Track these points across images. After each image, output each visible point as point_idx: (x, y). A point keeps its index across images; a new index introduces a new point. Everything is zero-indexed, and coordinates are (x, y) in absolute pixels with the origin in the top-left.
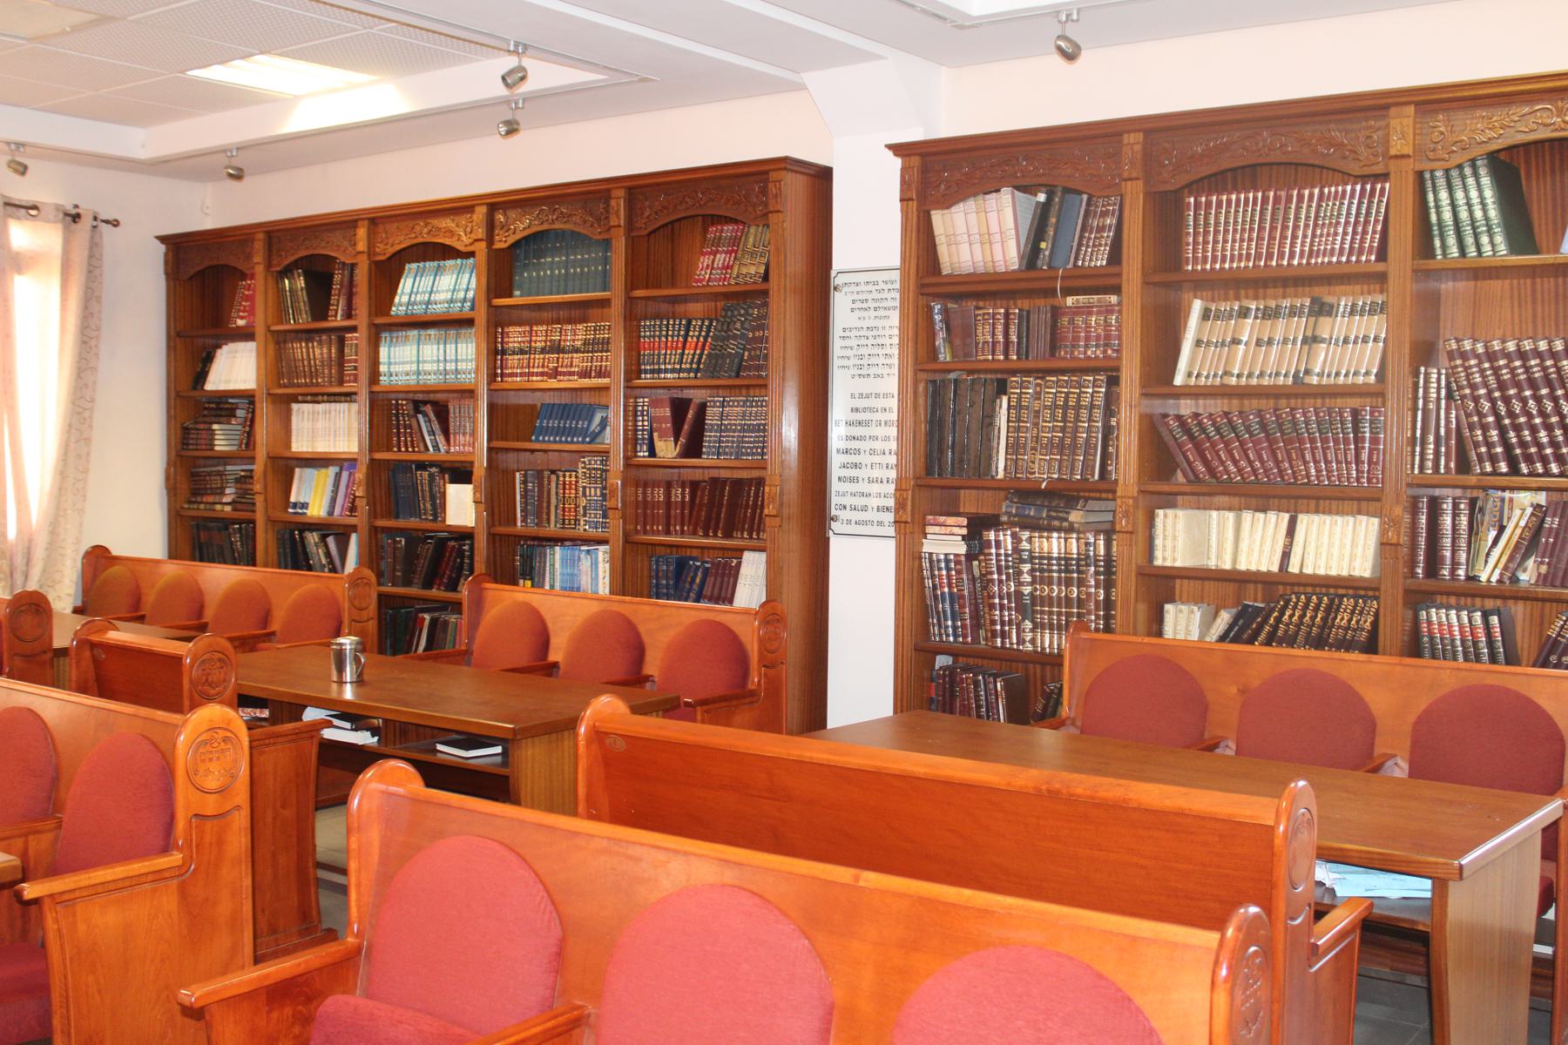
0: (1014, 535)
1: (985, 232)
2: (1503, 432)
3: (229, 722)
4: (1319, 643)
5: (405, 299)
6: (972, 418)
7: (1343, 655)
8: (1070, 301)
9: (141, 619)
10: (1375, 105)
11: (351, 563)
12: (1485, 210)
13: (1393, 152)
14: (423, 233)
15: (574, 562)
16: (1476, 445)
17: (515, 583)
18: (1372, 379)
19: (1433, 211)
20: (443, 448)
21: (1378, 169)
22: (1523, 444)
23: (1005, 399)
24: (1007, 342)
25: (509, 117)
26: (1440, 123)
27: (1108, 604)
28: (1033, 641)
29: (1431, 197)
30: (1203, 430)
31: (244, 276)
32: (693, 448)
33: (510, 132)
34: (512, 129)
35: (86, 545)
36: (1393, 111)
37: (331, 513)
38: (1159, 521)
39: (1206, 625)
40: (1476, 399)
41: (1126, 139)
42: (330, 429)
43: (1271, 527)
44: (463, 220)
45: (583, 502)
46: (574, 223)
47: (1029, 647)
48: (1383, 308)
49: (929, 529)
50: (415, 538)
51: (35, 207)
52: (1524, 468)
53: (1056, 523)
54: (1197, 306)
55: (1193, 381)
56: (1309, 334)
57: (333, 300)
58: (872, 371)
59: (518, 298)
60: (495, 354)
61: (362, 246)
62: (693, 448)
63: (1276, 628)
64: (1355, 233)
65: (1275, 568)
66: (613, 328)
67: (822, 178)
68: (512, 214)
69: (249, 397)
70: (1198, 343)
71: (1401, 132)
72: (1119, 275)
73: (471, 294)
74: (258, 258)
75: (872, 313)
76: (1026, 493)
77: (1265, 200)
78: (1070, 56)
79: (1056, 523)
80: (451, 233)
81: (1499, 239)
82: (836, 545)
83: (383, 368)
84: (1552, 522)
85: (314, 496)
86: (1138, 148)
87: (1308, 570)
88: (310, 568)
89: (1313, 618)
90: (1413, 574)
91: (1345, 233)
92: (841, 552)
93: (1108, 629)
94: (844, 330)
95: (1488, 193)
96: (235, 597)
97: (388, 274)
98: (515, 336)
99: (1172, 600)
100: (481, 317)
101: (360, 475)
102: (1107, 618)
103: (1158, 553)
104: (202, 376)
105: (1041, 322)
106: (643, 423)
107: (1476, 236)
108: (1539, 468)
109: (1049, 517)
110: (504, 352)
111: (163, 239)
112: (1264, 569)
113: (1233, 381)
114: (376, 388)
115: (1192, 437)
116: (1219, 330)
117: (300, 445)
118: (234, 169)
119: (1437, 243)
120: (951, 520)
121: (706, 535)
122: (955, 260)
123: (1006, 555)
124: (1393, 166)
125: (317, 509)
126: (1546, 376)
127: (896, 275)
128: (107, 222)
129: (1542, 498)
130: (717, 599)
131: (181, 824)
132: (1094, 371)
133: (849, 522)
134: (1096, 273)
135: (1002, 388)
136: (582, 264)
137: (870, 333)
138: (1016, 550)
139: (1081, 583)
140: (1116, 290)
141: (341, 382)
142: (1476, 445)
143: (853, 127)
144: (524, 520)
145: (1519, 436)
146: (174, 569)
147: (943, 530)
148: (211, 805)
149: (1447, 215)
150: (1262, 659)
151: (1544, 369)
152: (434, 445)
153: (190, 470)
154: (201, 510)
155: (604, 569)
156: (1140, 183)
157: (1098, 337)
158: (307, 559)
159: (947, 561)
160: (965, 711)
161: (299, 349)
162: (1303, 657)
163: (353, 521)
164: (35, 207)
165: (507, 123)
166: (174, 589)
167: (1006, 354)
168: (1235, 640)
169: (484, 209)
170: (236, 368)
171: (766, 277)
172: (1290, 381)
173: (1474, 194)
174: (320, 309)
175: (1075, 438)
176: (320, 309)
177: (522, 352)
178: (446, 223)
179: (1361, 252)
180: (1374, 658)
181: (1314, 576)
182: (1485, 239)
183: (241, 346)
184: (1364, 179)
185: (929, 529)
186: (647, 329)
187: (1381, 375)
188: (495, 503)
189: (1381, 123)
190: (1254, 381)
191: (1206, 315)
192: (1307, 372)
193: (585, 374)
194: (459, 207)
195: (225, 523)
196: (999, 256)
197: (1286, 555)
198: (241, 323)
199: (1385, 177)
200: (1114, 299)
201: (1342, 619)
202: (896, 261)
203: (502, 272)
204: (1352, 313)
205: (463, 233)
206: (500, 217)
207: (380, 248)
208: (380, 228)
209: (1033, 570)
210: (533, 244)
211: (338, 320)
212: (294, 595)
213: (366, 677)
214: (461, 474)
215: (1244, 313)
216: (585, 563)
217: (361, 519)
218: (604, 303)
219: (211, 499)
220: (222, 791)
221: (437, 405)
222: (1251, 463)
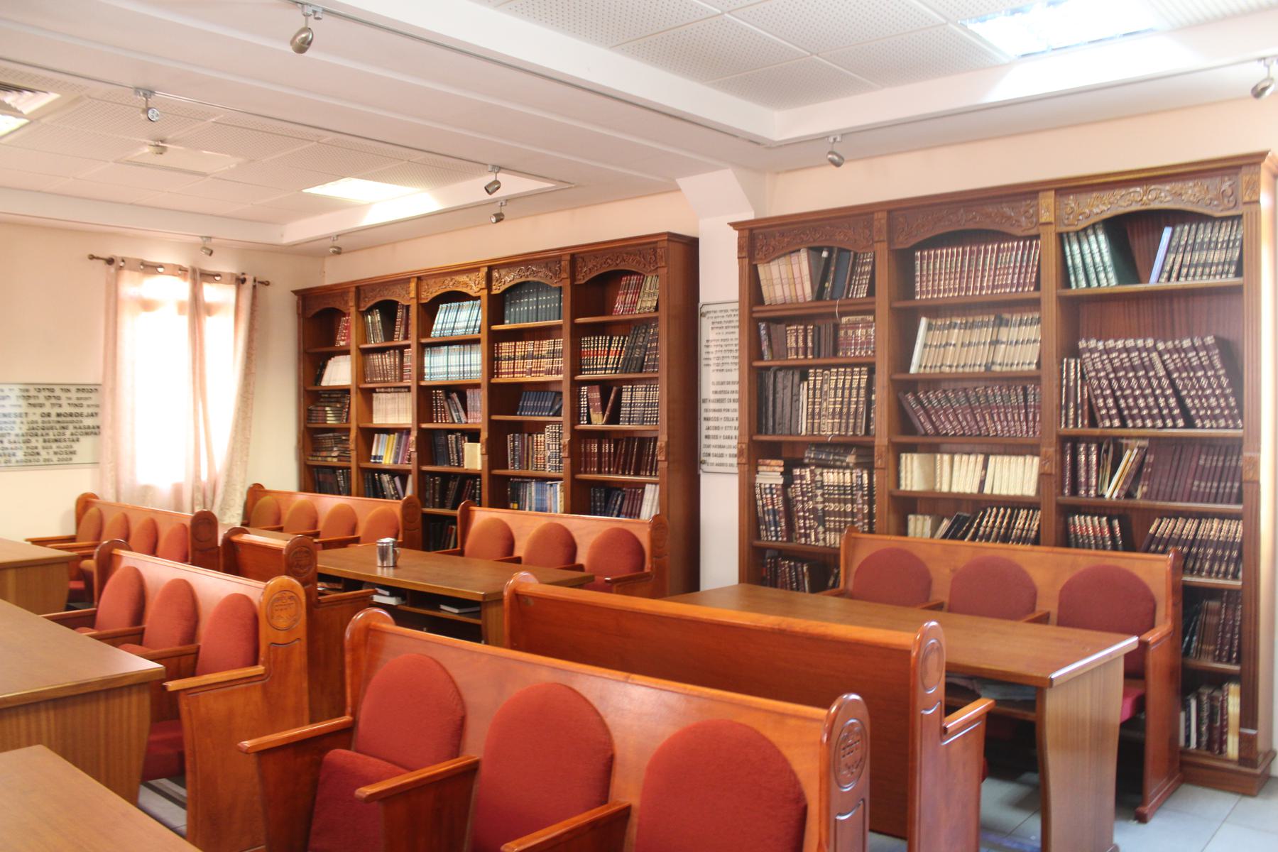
0: (812, 472)
1: (789, 279)
2: (1116, 400)
3: (293, 586)
4: (1005, 538)
5: (439, 327)
6: (784, 396)
7: (1020, 546)
8: (844, 320)
9: (281, 530)
10: (1027, 193)
11: (409, 492)
13: (1043, 220)
14: (450, 285)
15: (541, 492)
16: (1099, 409)
17: (507, 507)
18: (1033, 367)
20: (464, 420)
21: (1033, 232)
22: (1129, 408)
25: (498, 211)
26: (1071, 201)
27: (871, 515)
28: (824, 539)
29: (1067, 249)
31: (344, 315)
32: (614, 418)
33: (497, 221)
34: (500, 218)
35: (250, 483)
36: (1041, 195)
37: (396, 462)
38: (903, 460)
39: (935, 528)
41: (876, 216)
42: (395, 411)
43: (972, 465)
44: (473, 276)
45: (548, 453)
46: (541, 276)
47: (821, 543)
48: (1039, 321)
49: (760, 468)
50: (446, 476)
51: (218, 275)
52: (1130, 423)
54: (924, 322)
55: (922, 370)
57: (397, 328)
58: (725, 367)
59: (507, 326)
60: (492, 362)
61: (413, 294)
62: (614, 418)
63: (977, 529)
64: (1020, 273)
65: (975, 491)
66: (563, 343)
67: (690, 246)
68: (503, 272)
69: (345, 391)
70: (925, 346)
71: (1047, 207)
72: (873, 303)
73: (478, 323)
74: (352, 303)
75: (725, 330)
76: (820, 445)
77: (964, 253)
78: (837, 165)
80: (467, 285)
81: (1111, 275)
82: (705, 481)
83: (427, 371)
84: (1150, 458)
85: (385, 453)
86: (884, 221)
87: (996, 492)
88: (384, 497)
89: (1002, 523)
90: (1063, 494)
91: (1014, 273)
92: (709, 485)
93: (871, 531)
95: (1104, 246)
96: (338, 513)
97: (429, 311)
98: (506, 348)
99: (915, 512)
100: (484, 337)
101: (413, 438)
102: (871, 524)
103: (903, 482)
104: (320, 377)
105: (827, 330)
106: (584, 403)
107: (1097, 274)
108: (1139, 422)
110: (499, 359)
111: (296, 292)
112: (968, 491)
113: (947, 370)
114: (423, 383)
115: (923, 407)
116: (938, 337)
117: (378, 420)
118: (337, 248)
119: (1072, 278)
120: (774, 462)
121: (623, 474)
124: (1042, 230)
125: (387, 461)
126: (1143, 363)
127: (736, 306)
128: (262, 283)
129: (1145, 443)
130: (630, 515)
131: (263, 648)
132: (860, 365)
134: (861, 302)
136: (547, 302)
138: (813, 481)
139: (853, 502)
140: (872, 312)
141: (402, 379)
142: (1099, 409)
143: (712, 211)
144: (513, 464)
146: (304, 497)
148: (281, 638)
149: (1078, 260)
150: (966, 550)
151: (1141, 359)
152: (457, 419)
153: (312, 437)
154: (318, 461)
155: (560, 496)
156: (885, 245)
157: (862, 343)
158: (383, 491)
159: (771, 489)
160: (784, 586)
161: (376, 359)
162: (995, 549)
163: (409, 467)
164: (218, 275)
165: (496, 215)
166: (301, 509)
167: (805, 354)
168: (953, 537)
169: (486, 270)
170: (339, 373)
171: (657, 309)
172: (983, 369)
173: (1094, 246)
174: (389, 333)
175: (849, 409)
176: (389, 333)
177: (509, 359)
178: (463, 278)
179: (1024, 286)
180: (1036, 548)
181: (1000, 496)
182: (1102, 275)
183: (341, 358)
184: (1025, 238)
185: (760, 468)
186: (588, 343)
187: (1038, 364)
188: (496, 455)
189: (1034, 203)
190: (960, 370)
191: (929, 327)
192: (993, 363)
193: (549, 372)
194: (471, 269)
195: (334, 469)
196: (800, 293)
197: (982, 483)
198: (342, 343)
199: (1037, 237)
200: (870, 318)
201: (1020, 523)
202: (736, 297)
203: (497, 307)
205: (473, 285)
206: (495, 274)
207: (424, 295)
208: (424, 283)
209: (823, 495)
210: (515, 291)
211: (399, 341)
212: (372, 514)
213: (399, 563)
214: (473, 436)
216: (549, 493)
217: (412, 466)
218: (559, 327)
219: (325, 454)
220: (288, 630)
221: (458, 391)
222: (977, 423)
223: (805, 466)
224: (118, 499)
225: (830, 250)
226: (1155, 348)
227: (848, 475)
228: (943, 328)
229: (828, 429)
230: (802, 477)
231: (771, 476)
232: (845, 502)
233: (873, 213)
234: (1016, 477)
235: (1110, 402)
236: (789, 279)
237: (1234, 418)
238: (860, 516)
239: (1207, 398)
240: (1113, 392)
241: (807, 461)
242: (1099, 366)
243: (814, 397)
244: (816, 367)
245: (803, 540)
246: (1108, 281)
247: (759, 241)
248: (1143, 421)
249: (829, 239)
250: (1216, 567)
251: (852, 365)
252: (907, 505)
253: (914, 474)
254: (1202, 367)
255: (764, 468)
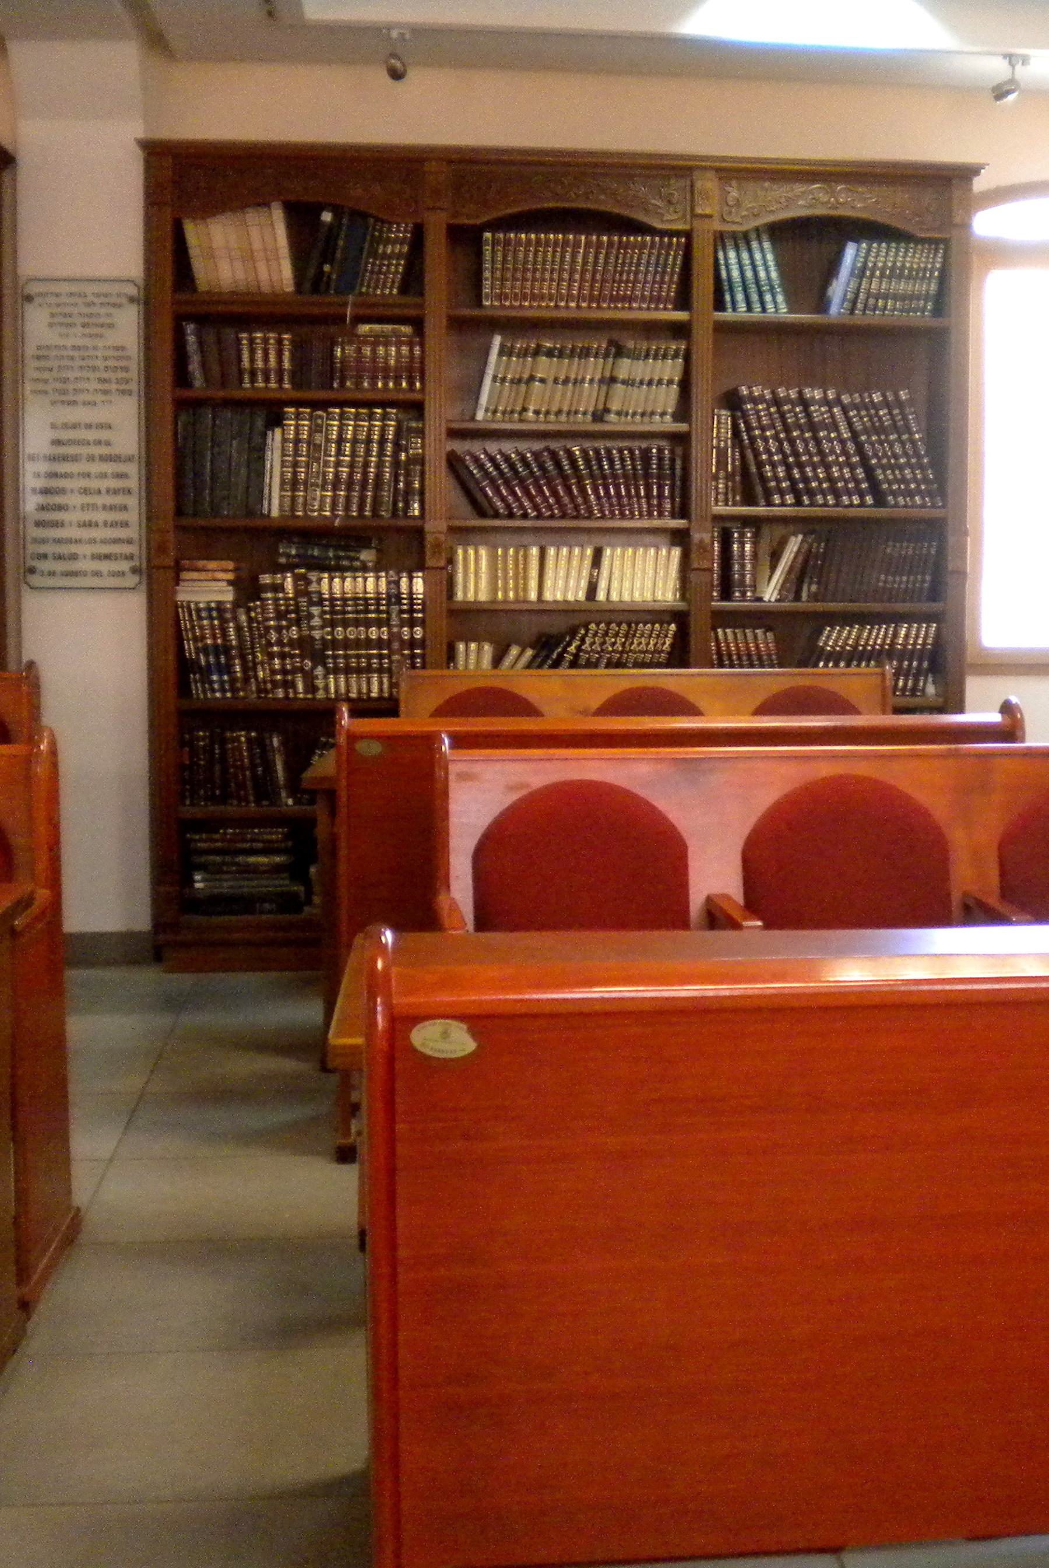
0: (297, 578)
1: (248, 252)
2: (789, 468)
8: (364, 328)
12: (768, 272)
19: (723, 267)
23: (278, 432)
24: (280, 371)
28: (326, 688)
30: (497, 467)
40: (766, 440)
41: (427, 167)
47: (320, 695)
49: (185, 575)
52: (806, 500)
53: (345, 563)
56: (607, 374)
58: (81, 398)
72: (421, 306)
79: (345, 563)
81: (780, 298)
94: (39, 348)
95: (770, 257)
107: (761, 295)
109: (338, 558)
116: (516, 367)
119: (728, 298)
122: (275, 278)
123: (287, 599)
133: (52, 574)
135: (276, 420)
137: (76, 354)
138: (298, 593)
139: (387, 623)
145: (802, 472)
147: (203, 575)
149: (735, 273)
167: (280, 381)
173: (758, 256)
175: (365, 474)
182: (768, 298)
192: (607, 410)
200: (406, 329)
204: (647, 356)
215: (536, 353)
223: (283, 569)
224: (184, 580)
225: (337, 211)
226: (838, 401)
227: (371, 582)
228: (524, 354)
229: (322, 505)
230: (278, 588)
231: (209, 588)
232: (368, 624)
233: (424, 160)
234: (643, 575)
235: (781, 472)
236: (248, 252)
237: (930, 493)
238: (396, 645)
239: (901, 468)
240: (785, 457)
241: (283, 560)
242: (765, 421)
243: (297, 453)
244: (298, 403)
245: (280, 693)
246: (778, 308)
247: (187, 180)
248: (782, 496)
249: (328, 194)
250: (901, 683)
251: (370, 404)
252: (470, 621)
253: (477, 574)
254: (895, 427)
255: (195, 575)
